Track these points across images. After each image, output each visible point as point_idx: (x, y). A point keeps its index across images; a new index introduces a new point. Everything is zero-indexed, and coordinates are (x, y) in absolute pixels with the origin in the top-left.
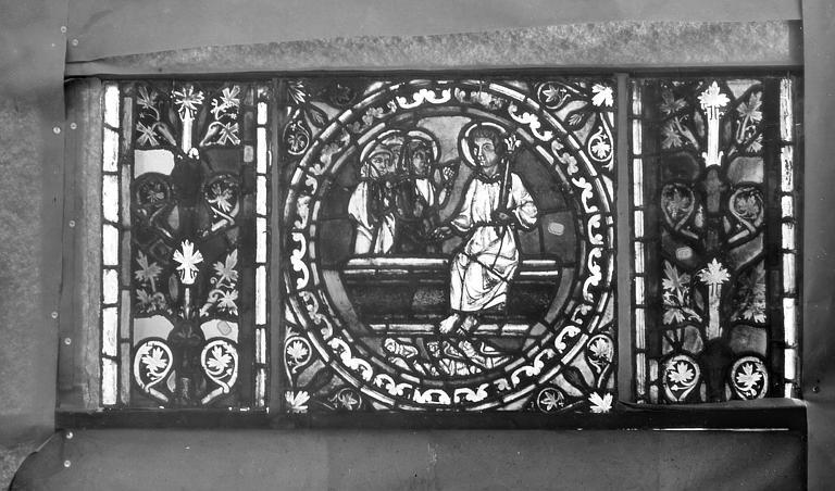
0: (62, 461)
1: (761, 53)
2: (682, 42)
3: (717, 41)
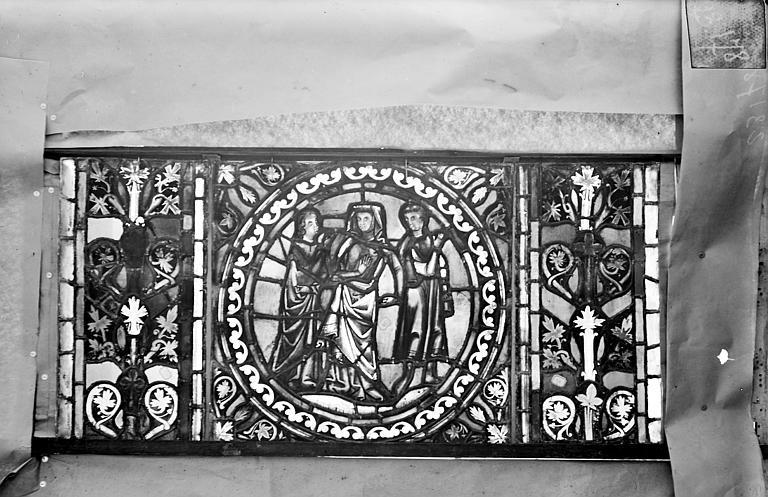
0: (38, 479)
2: (582, 129)
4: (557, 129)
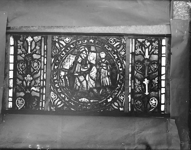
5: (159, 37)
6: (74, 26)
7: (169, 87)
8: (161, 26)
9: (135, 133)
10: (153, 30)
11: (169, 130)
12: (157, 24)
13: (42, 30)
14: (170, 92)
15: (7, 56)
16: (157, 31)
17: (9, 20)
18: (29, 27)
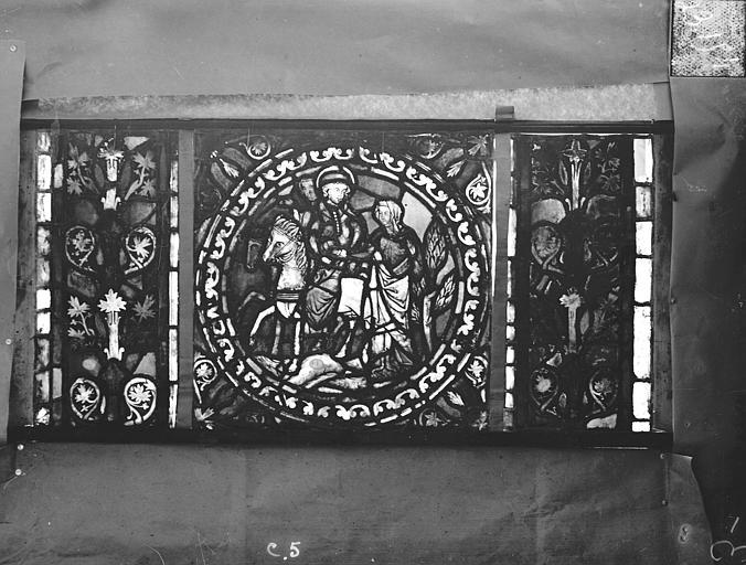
1: (628, 108)
3: (589, 98)
4: (534, 100)
5: (624, 134)
6: (290, 95)
7: (665, 327)
8: (635, 87)
9: (535, 511)
10: (602, 108)
11: (668, 495)
12: (617, 83)
13: (162, 110)
14: (669, 348)
15: (26, 216)
16: (616, 109)
17: (32, 73)
18: (111, 100)
